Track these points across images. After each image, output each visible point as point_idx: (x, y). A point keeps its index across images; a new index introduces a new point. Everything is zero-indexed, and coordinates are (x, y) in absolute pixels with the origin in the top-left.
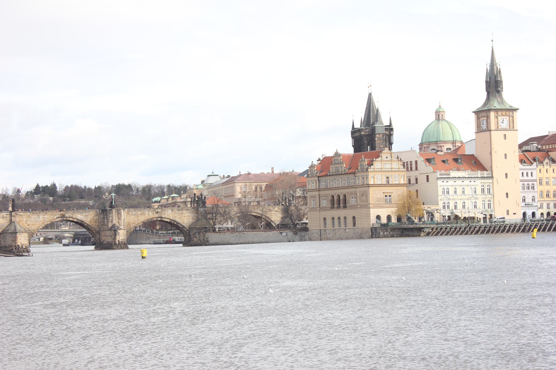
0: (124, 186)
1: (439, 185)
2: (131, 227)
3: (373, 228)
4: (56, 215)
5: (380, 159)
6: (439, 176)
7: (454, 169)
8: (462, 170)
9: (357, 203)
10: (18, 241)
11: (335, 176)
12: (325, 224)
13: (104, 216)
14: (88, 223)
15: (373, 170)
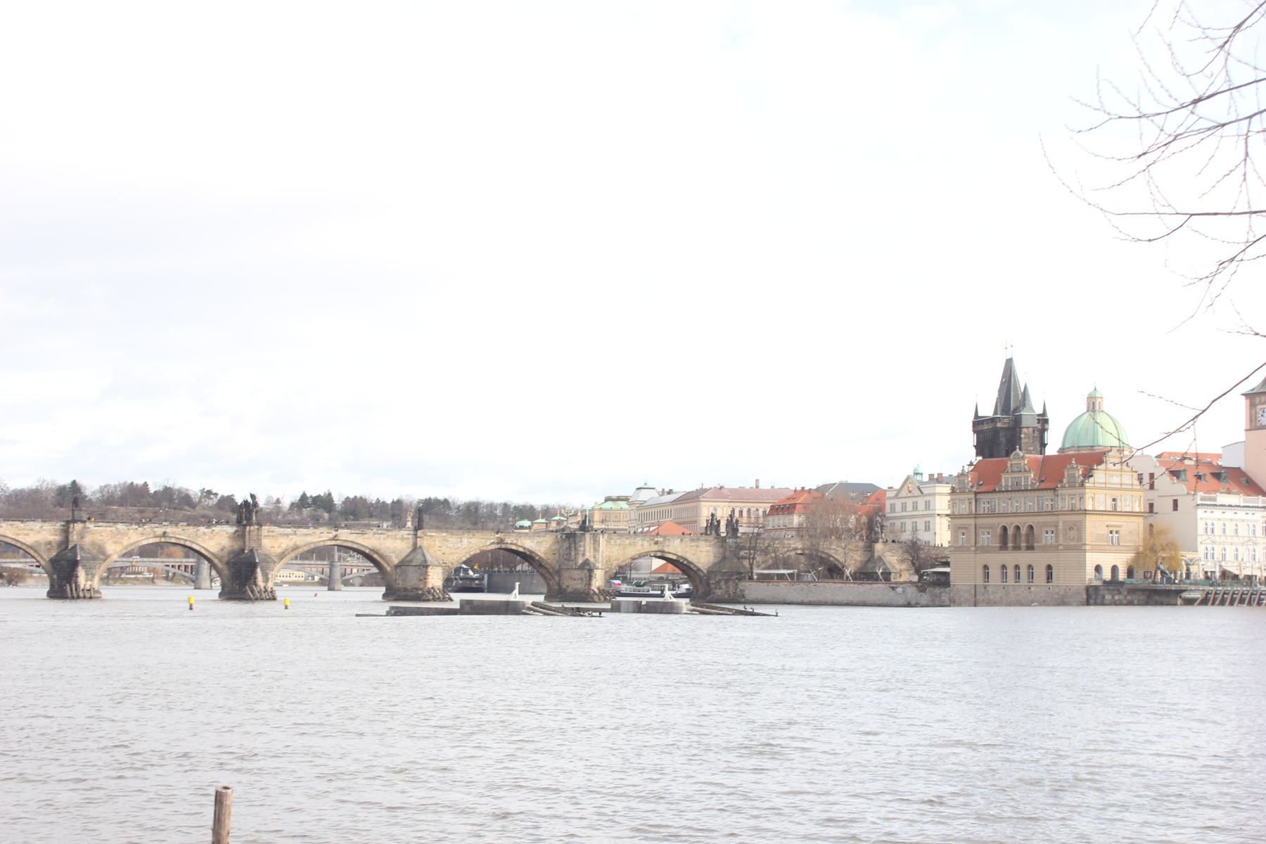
0: (437, 502)
1: (1199, 517)
2: (612, 565)
3: (1091, 586)
4: (490, 539)
5: (1103, 466)
6: (1199, 502)
7: (1222, 490)
8: (1234, 493)
9: (1057, 541)
10: (429, 581)
11: (1013, 493)
12: (987, 576)
13: (570, 544)
14: (542, 555)
15: (1093, 485)
